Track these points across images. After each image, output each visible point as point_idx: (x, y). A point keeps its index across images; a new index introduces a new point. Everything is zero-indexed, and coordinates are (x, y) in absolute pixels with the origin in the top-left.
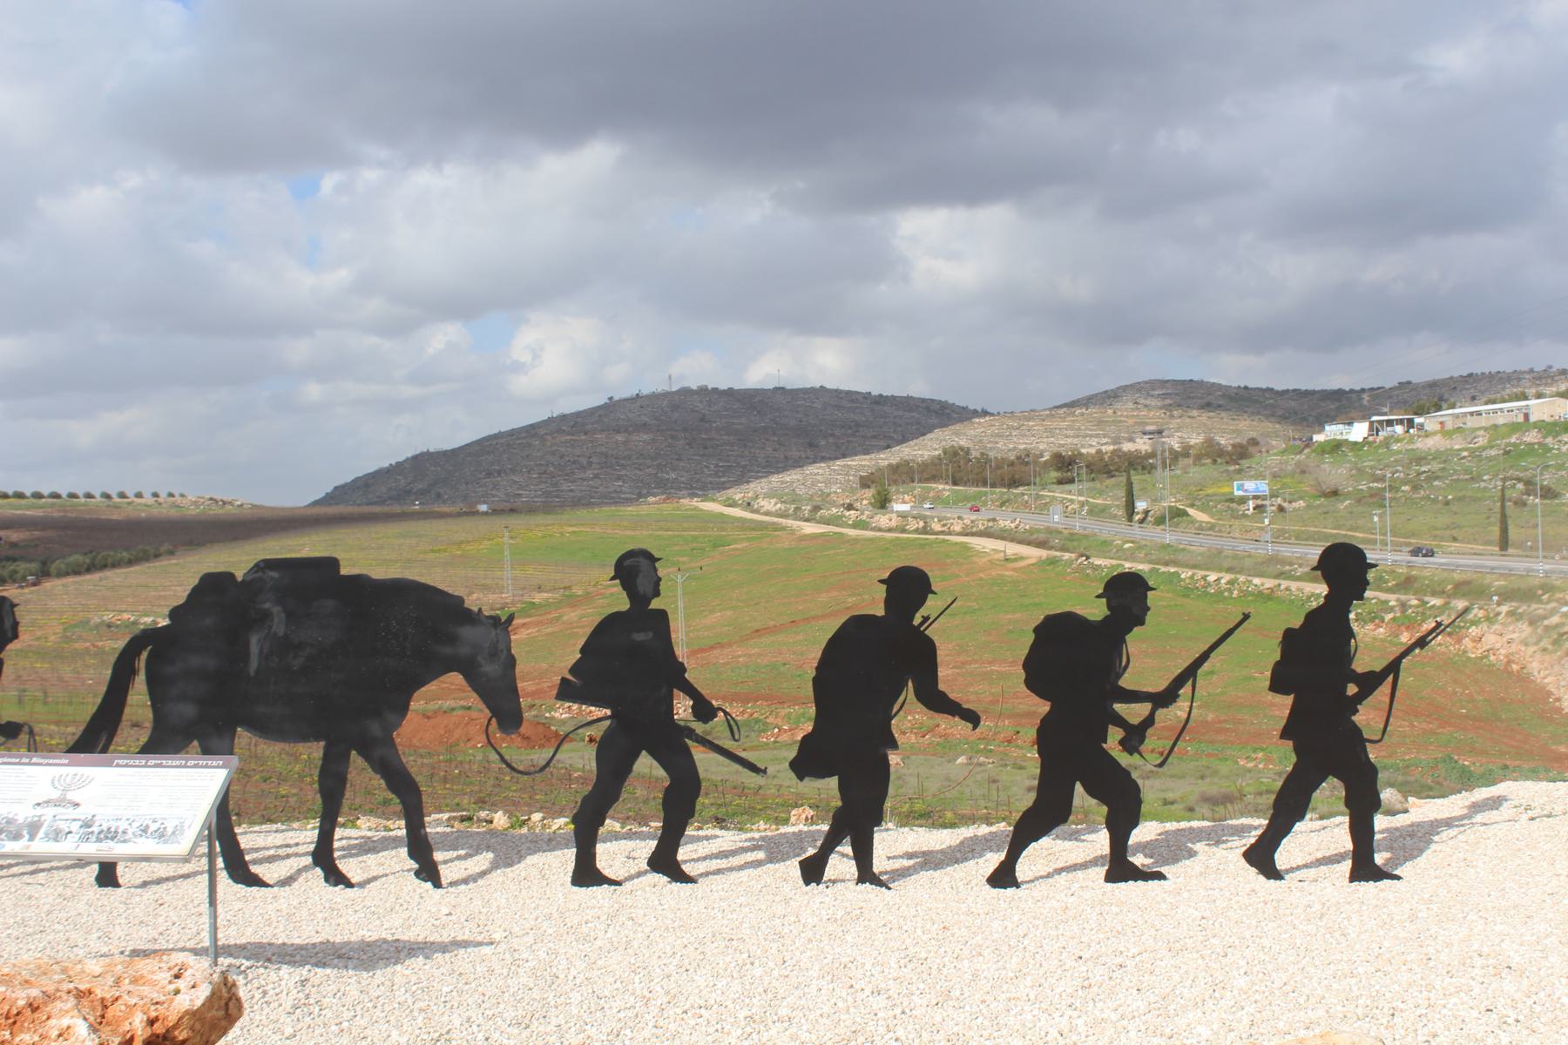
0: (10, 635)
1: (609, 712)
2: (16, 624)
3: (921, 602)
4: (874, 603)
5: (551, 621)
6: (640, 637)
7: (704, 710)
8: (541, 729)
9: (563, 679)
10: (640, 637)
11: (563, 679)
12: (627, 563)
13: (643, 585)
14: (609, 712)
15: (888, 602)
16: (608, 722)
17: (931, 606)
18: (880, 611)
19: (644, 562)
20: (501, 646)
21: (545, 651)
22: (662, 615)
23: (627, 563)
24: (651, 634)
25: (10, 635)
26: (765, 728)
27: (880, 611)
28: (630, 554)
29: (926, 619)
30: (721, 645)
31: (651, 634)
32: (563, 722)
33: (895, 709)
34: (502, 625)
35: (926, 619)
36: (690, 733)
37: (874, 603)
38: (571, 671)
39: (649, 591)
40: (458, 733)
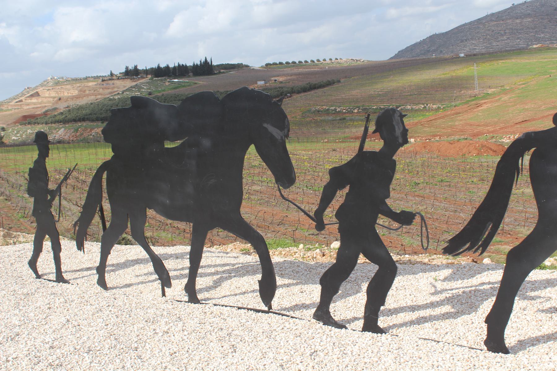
0: (400, 140)
2: (405, 132)
8: (501, 147)
25: (400, 140)
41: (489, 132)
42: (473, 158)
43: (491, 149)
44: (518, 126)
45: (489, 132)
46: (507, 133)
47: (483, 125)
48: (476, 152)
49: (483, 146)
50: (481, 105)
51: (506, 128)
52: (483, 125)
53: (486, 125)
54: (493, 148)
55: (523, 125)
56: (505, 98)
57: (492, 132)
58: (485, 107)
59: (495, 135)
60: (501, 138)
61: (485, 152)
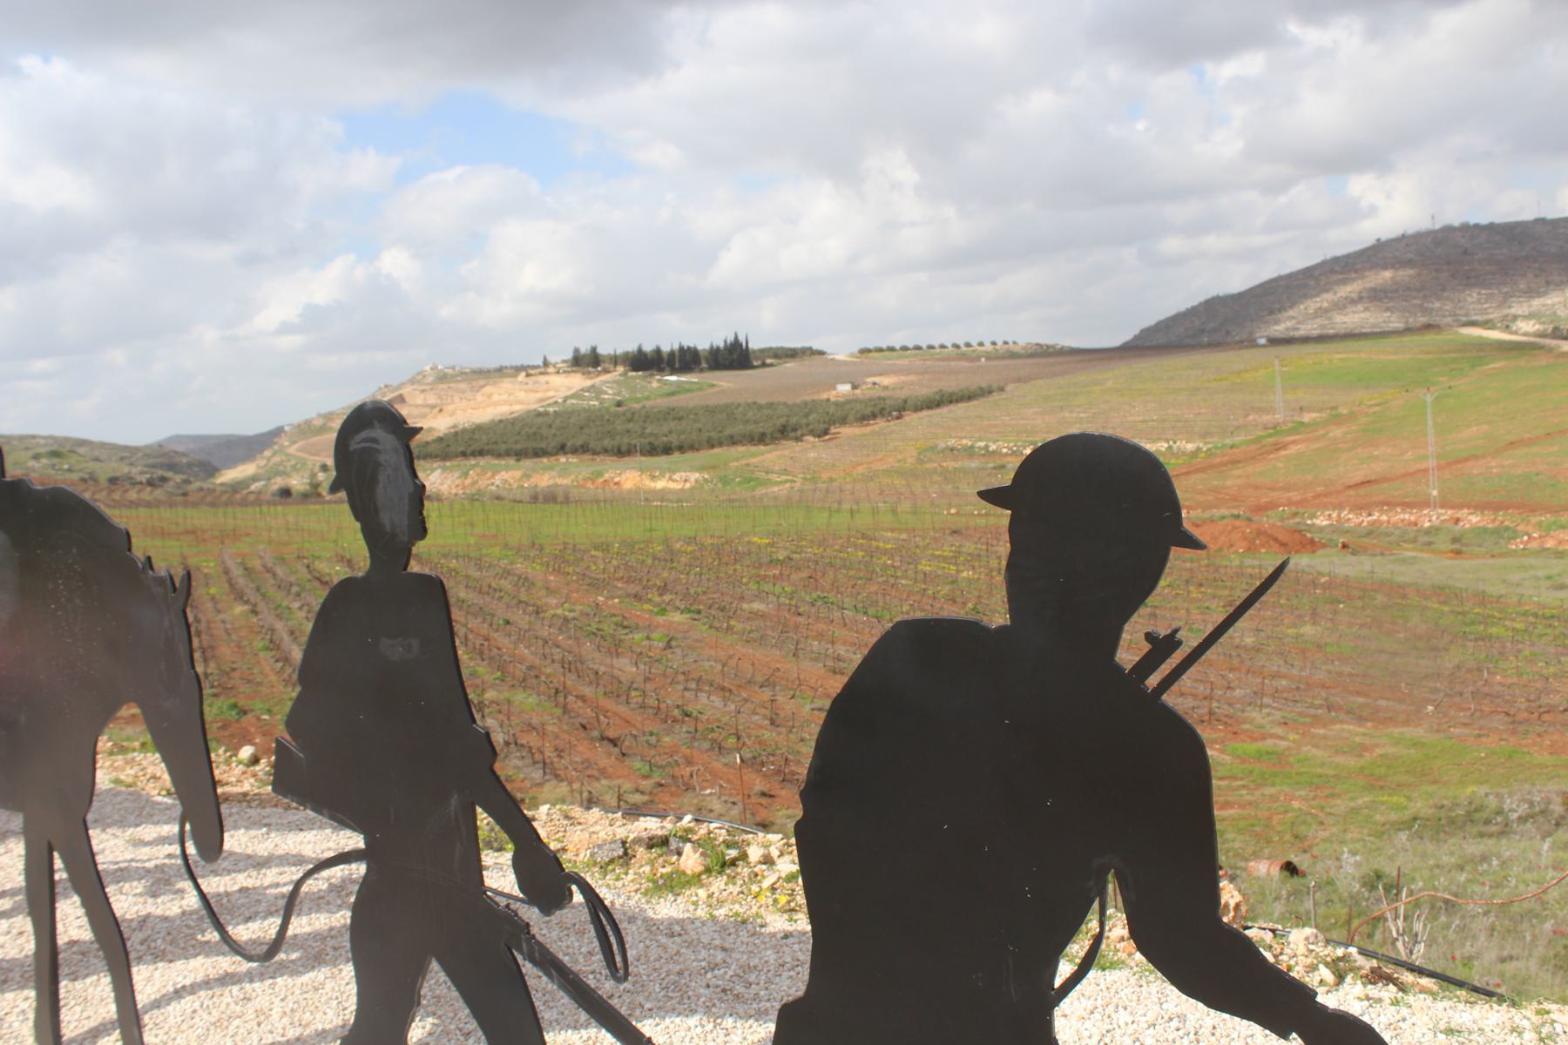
1: (356, 841)
3: (1139, 582)
4: (972, 581)
5: (1317, 439)
6: (394, 650)
8: (1297, 536)
10: (394, 650)
12: (354, 445)
15: (1016, 572)
17: (1179, 601)
18: (998, 616)
22: (434, 590)
24: (415, 643)
26: (1515, 534)
27: (998, 616)
29: (1161, 646)
30: (1475, 457)
32: (1321, 529)
33: (1065, 970)
35: (1161, 646)
37: (972, 581)
40: (1222, 539)
41: (1290, 503)
43: (1276, 540)
44: (1352, 492)
45: (1290, 503)
46: (1325, 507)
47: (1282, 489)
49: (1260, 533)
50: (1284, 446)
51: (1326, 495)
52: (1282, 489)
54: (1281, 537)
55: (1362, 491)
56: (1337, 432)
57: (1298, 503)
58: (1293, 450)
59: (1301, 510)
60: (1313, 516)
61: (1263, 546)
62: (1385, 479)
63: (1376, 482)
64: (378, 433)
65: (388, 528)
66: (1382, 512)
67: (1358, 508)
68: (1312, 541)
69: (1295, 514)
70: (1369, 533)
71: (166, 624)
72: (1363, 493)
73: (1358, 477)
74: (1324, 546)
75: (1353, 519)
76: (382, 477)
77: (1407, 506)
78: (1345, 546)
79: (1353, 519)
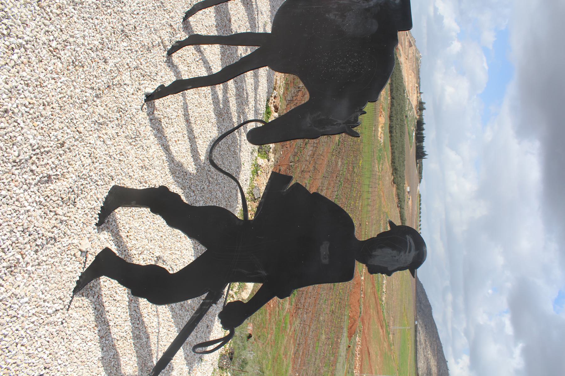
1: (251, 217)
5: (384, 339)
7: (234, 315)
9: (290, 178)
10: (324, 249)
11: (290, 178)
12: (409, 239)
13: (382, 255)
14: (251, 217)
16: (238, 212)
19: (410, 256)
20: (329, 129)
21: (318, 166)
22: (347, 275)
23: (409, 239)
24: (326, 261)
28: (420, 243)
31: (326, 261)
32: (355, 339)
34: (350, 128)
36: (214, 298)
38: (297, 184)
39: (375, 262)
40: (353, 309)
41: (364, 329)
42: (347, 312)
43: (353, 326)
45: (364, 329)
46: (362, 340)
47: (369, 327)
48: (352, 316)
49: (355, 321)
50: (382, 328)
51: (366, 340)
52: (369, 327)
53: (369, 329)
55: (366, 352)
57: (364, 332)
58: (381, 331)
62: (370, 359)
63: (369, 356)
64: (413, 253)
65: (374, 253)
66: (360, 358)
67: (361, 351)
68: (351, 337)
69: (360, 331)
70: (353, 354)
71: (340, 121)
72: (366, 353)
73: (371, 351)
74: (350, 340)
75: (358, 349)
76: (395, 252)
77: (361, 366)
78: (349, 346)
79: (358, 349)
